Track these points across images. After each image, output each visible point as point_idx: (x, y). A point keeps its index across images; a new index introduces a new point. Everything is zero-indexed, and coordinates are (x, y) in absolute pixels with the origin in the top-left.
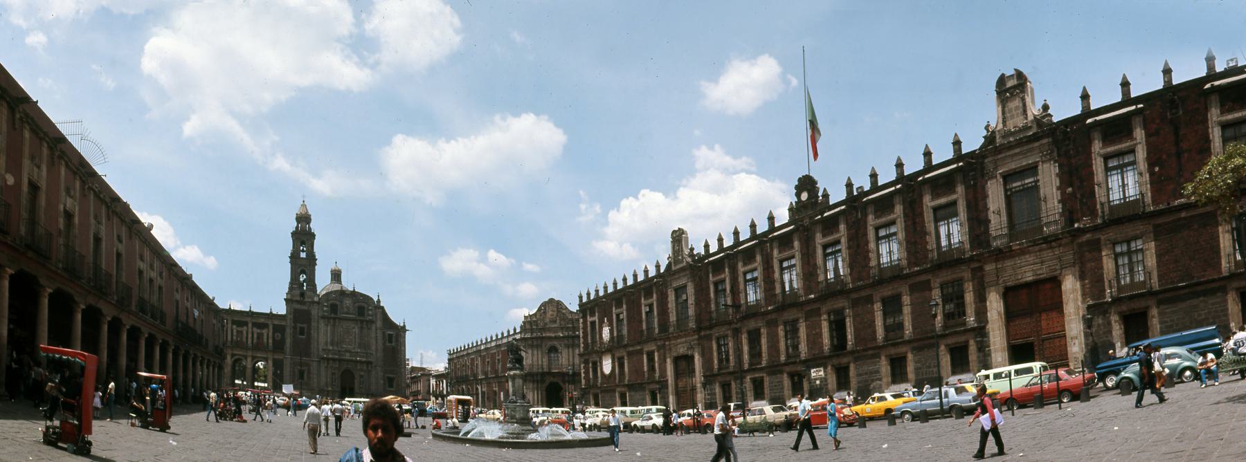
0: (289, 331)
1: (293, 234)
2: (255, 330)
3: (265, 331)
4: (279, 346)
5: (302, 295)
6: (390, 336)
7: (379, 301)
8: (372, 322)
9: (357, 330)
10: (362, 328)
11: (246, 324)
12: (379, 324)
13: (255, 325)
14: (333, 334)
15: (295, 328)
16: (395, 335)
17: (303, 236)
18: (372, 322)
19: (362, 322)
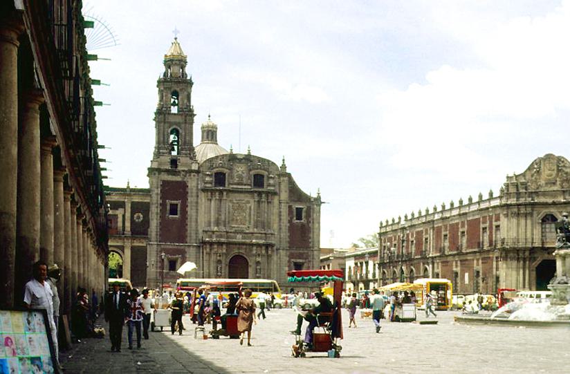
1: (159, 82)
5: (174, 162)
6: (299, 211)
7: (284, 167)
8: (275, 194)
9: (252, 204)
12: (284, 195)
14: (219, 211)
15: (163, 205)
16: (303, 212)
18: (275, 194)
19: (260, 194)
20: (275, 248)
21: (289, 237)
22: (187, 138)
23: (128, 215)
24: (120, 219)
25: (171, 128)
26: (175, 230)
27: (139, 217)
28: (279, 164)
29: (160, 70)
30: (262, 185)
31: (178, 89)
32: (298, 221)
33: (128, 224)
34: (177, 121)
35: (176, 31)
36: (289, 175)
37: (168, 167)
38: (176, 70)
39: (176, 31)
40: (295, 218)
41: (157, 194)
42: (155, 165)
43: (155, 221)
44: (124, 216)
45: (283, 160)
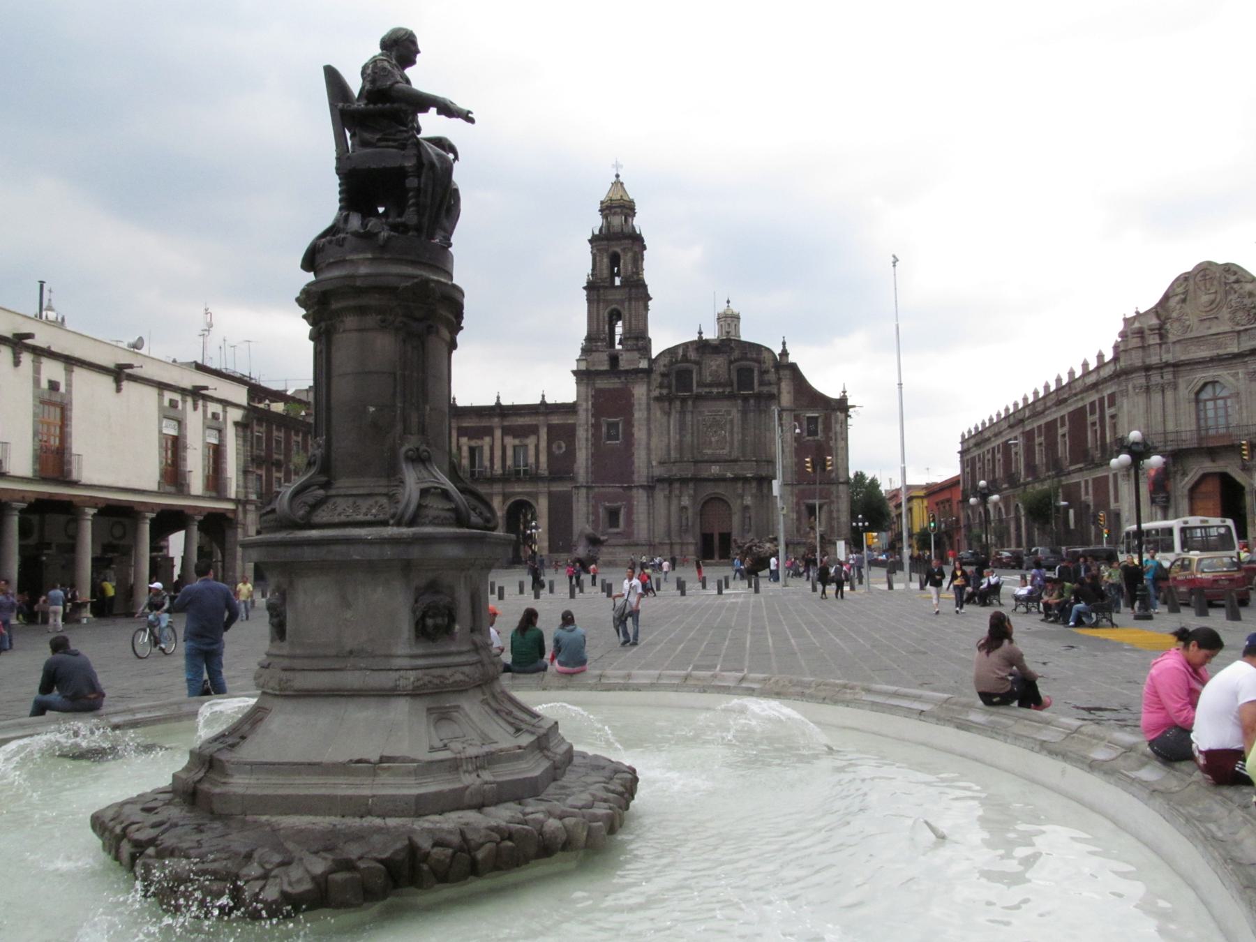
0: (582, 435)
1: (594, 240)
2: (510, 441)
3: (531, 441)
4: (561, 469)
5: (614, 359)
7: (785, 353)
9: (735, 414)
10: (744, 413)
11: (489, 431)
12: (786, 399)
13: (506, 431)
14: (682, 427)
15: (596, 426)
23: (543, 444)
24: (532, 452)
26: (614, 464)
27: (561, 448)
28: (777, 350)
29: (596, 222)
31: (618, 250)
33: (543, 459)
34: (618, 297)
35: (617, 166)
36: (794, 368)
37: (605, 367)
38: (617, 221)
39: (617, 166)
41: (587, 410)
42: (583, 366)
43: (584, 451)
44: (537, 447)
45: (784, 344)
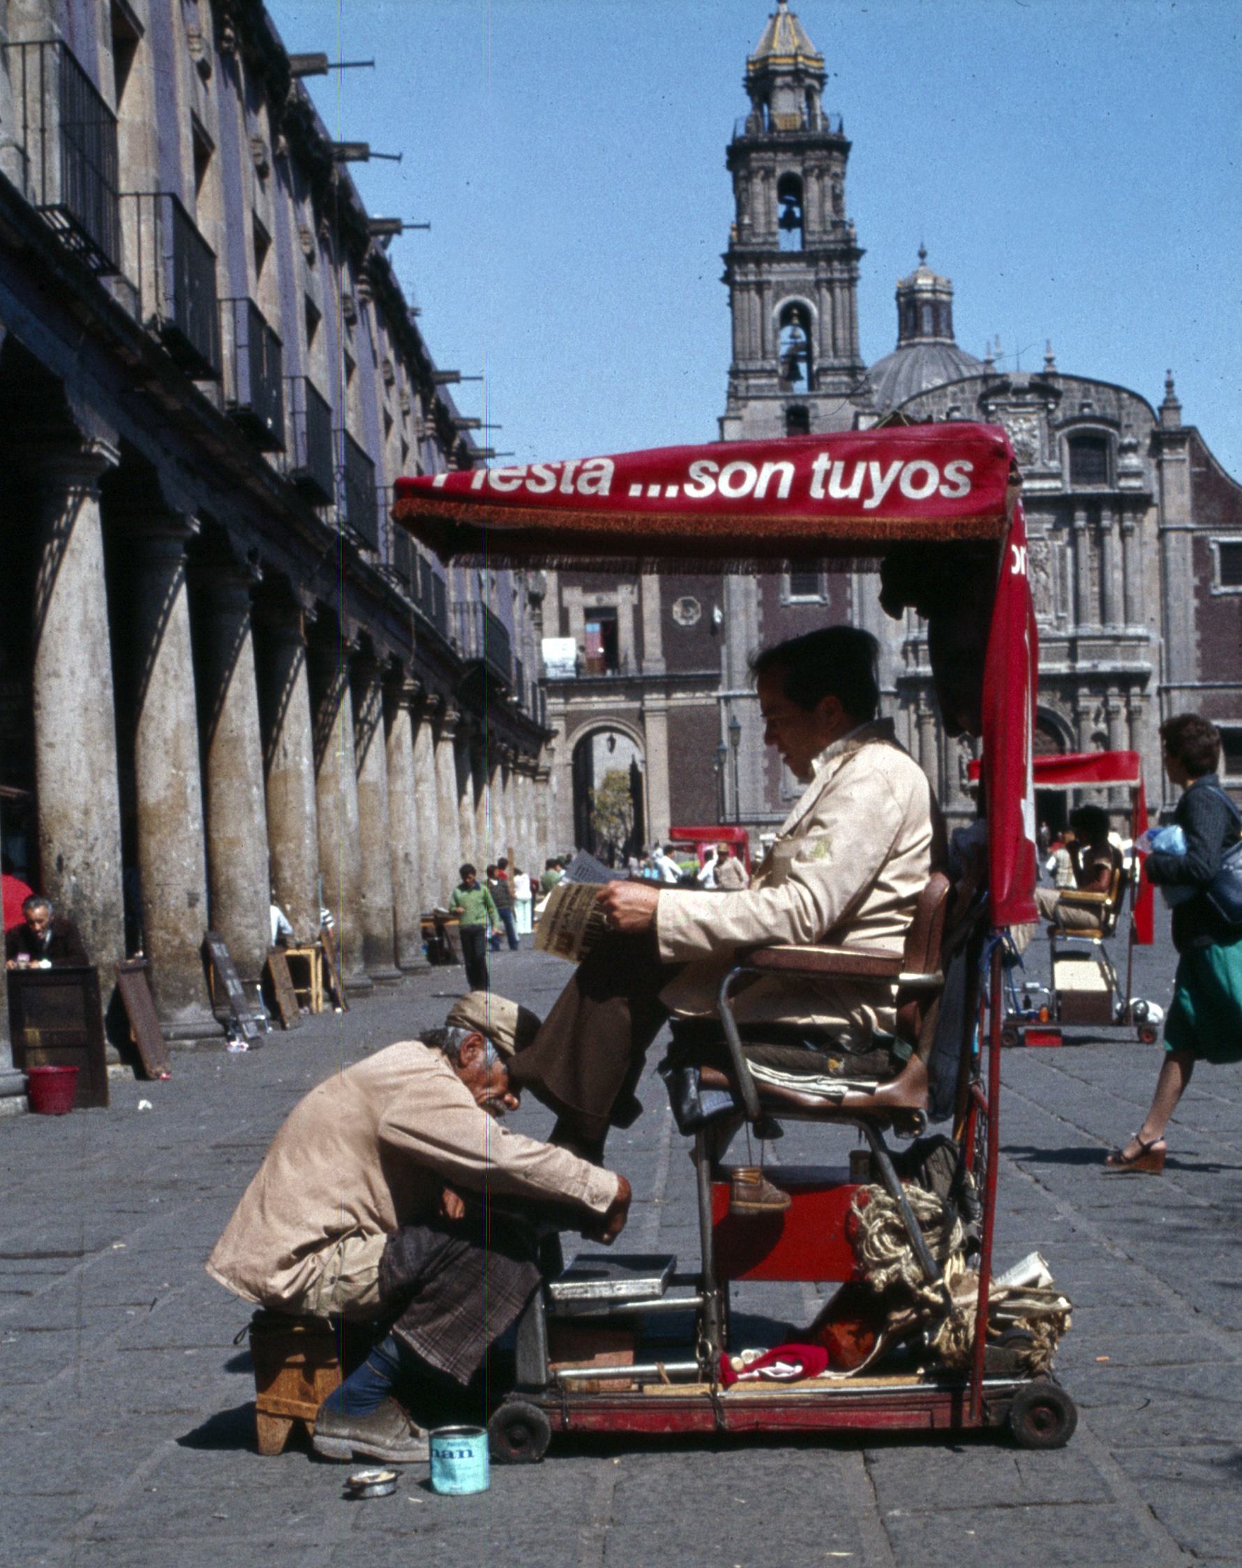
7: (1171, 405)
8: (1140, 503)
12: (1178, 502)
17: (785, 150)
18: (1140, 503)
19: (1094, 505)
20: (1153, 685)
21: (1199, 645)
22: (840, 333)
23: (652, 605)
25: (779, 306)
28: (1156, 399)
30: (1102, 473)
31: (797, 170)
32: (1229, 589)
33: (653, 637)
36: (1188, 436)
37: (778, 433)
40: (1218, 579)
44: (638, 611)
45: (1169, 385)
